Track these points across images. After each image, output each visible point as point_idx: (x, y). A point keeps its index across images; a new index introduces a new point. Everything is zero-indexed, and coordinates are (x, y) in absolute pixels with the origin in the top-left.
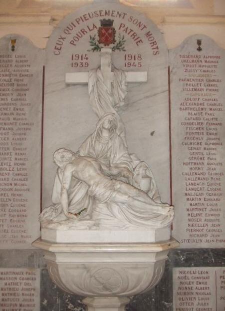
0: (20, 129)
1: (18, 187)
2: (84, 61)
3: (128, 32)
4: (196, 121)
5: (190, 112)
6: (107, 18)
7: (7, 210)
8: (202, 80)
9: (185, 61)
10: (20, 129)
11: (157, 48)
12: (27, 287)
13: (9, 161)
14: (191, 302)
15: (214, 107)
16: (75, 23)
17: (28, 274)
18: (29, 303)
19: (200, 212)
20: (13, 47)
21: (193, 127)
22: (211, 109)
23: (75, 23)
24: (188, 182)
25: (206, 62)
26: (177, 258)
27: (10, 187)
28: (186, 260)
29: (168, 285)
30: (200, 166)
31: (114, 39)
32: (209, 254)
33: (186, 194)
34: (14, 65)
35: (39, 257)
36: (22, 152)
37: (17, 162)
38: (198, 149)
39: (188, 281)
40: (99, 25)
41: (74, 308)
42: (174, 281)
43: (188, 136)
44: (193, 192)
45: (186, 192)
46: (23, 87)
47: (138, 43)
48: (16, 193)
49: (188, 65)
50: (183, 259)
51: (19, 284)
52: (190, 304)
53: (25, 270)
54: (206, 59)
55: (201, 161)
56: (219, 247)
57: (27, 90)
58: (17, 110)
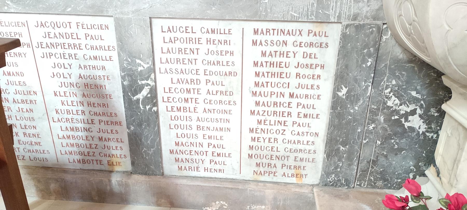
12: (308, 61)
17: (311, 35)
18: (310, 92)
41: (401, 105)
51: (291, 55)
53: (306, 27)
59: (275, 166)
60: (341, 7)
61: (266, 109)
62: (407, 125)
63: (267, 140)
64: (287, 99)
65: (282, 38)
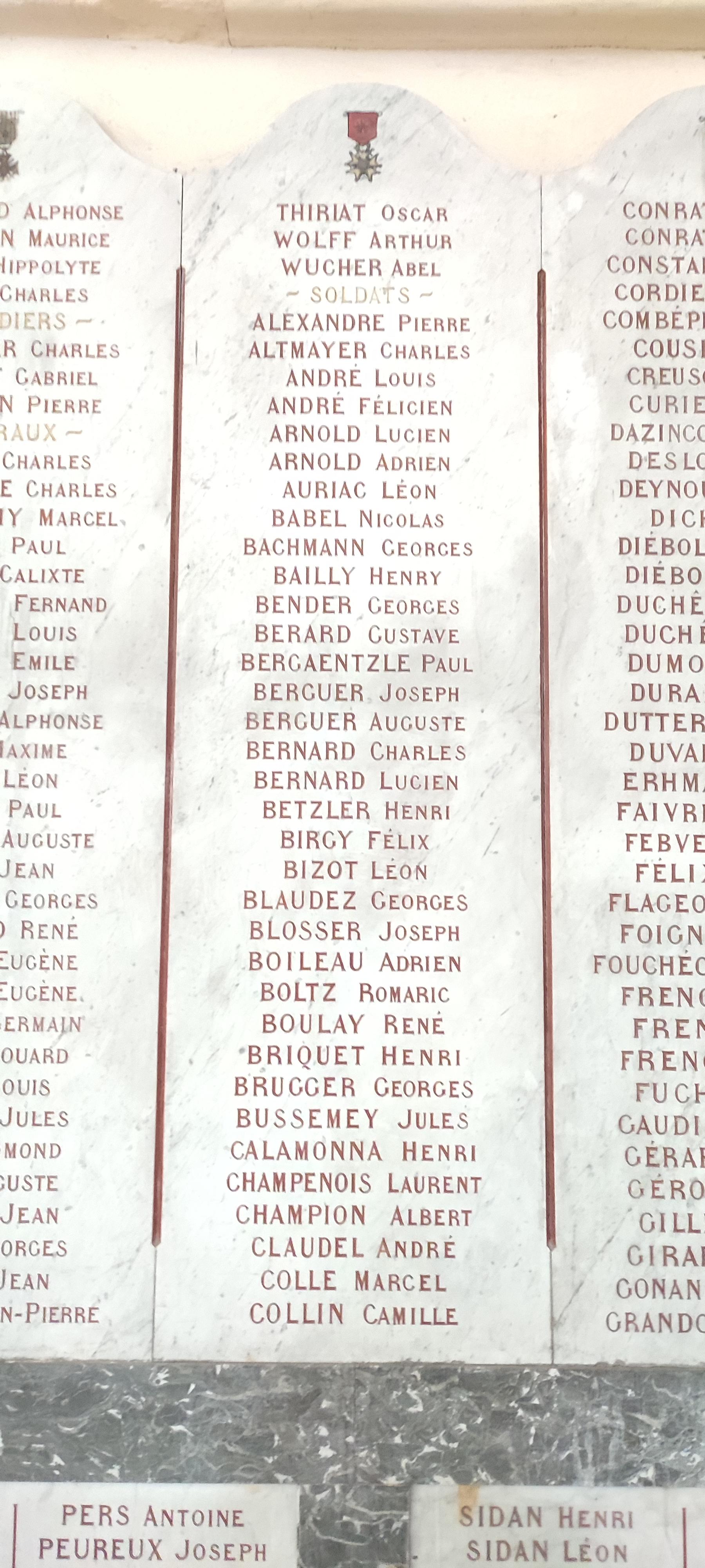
15: (61, 505)
22: (45, 518)
25: (35, 239)
54: (36, 225)
56: (43, 1356)
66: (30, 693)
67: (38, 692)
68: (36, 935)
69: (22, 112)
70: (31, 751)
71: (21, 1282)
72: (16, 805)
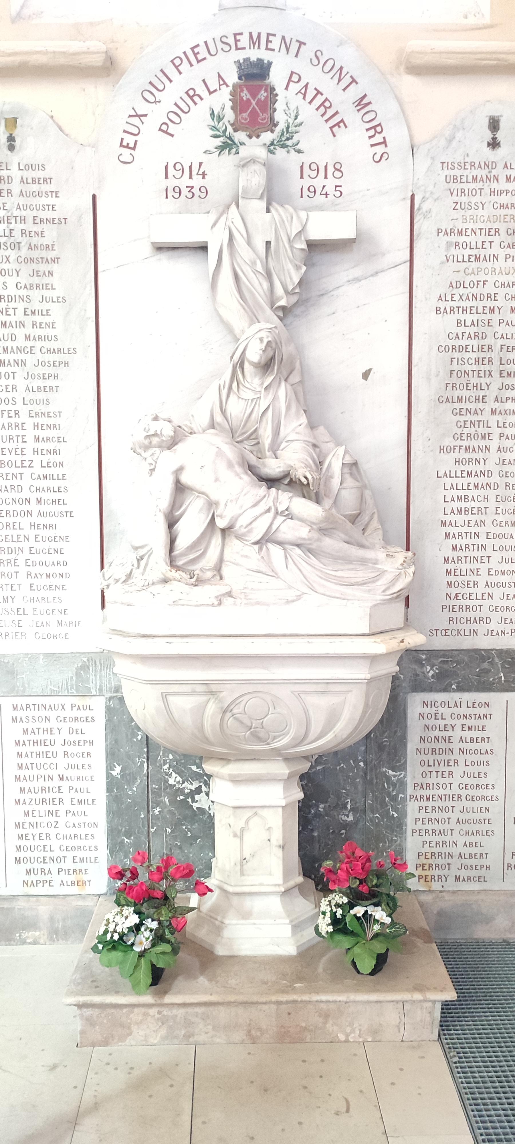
0: (44, 364)
1: (44, 508)
2: (197, 182)
3: (309, 97)
4: (475, 343)
5: (462, 317)
6: (254, 55)
7: (21, 562)
8: (497, 231)
9: (455, 178)
10: (44, 364)
11: (384, 142)
12: (74, 737)
13: (21, 445)
14: (447, 769)
16: (171, 71)
17: (75, 709)
18: (81, 773)
19: (475, 566)
20: (11, 139)
21: (467, 356)
23: (171, 71)
24: (449, 494)
26: (419, 671)
27: (26, 507)
28: (441, 676)
29: (396, 732)
30: (480, 455)
31: (272, 118)
32: (491, 663)
33: (444, 524)
34: (16, 191)
35: (101, 670)
36: (51, 421)
37: (41, 445)
38: (476, 413)
39: (442, 723)
40: (232, 78)
41: (183, 782)
42: (409, 722)
43: (454, 379)
44: (460, 519)
45: (444, 518)
46: (44, 254)
47: (334, 129)
48: (42, 521)
49: (463, 192)
50: (432, 672)
51: (56, 731)
52: (446, 774)
53: (68, 701)
55: (482, 443)
57: (55, 260)
58: (33, 313)
59: (50, 872)
60: (101, 680)
61: (33, 796)
62: (195, 806)
63: (37, 837)
64: (56, 783)
65: (44, 713)
66: (507, 387)
67: (511, 387)
68: (511, 488)
69: (502, 116)
70: (508, 412)
71: (508, 621)
72: (502, 435)
